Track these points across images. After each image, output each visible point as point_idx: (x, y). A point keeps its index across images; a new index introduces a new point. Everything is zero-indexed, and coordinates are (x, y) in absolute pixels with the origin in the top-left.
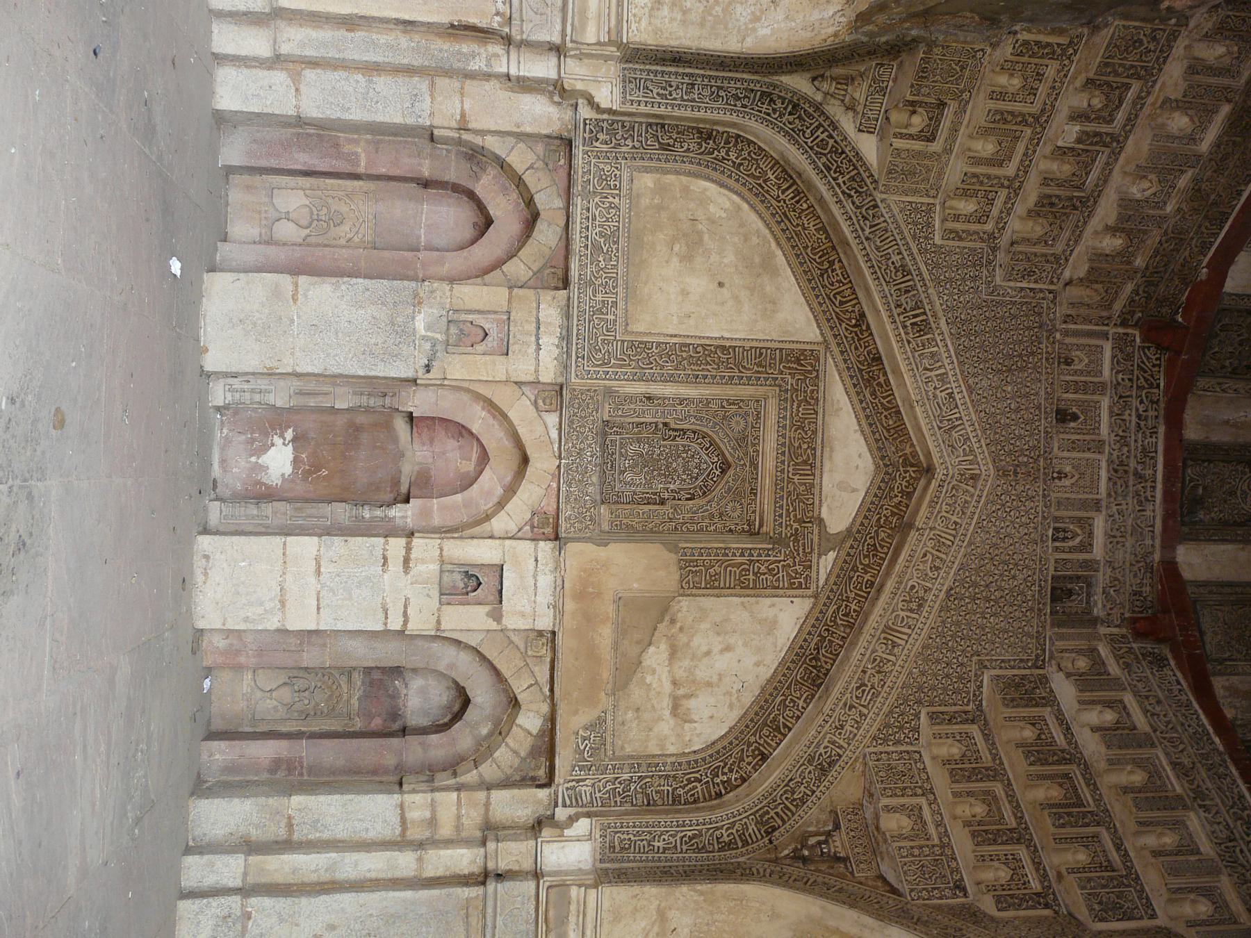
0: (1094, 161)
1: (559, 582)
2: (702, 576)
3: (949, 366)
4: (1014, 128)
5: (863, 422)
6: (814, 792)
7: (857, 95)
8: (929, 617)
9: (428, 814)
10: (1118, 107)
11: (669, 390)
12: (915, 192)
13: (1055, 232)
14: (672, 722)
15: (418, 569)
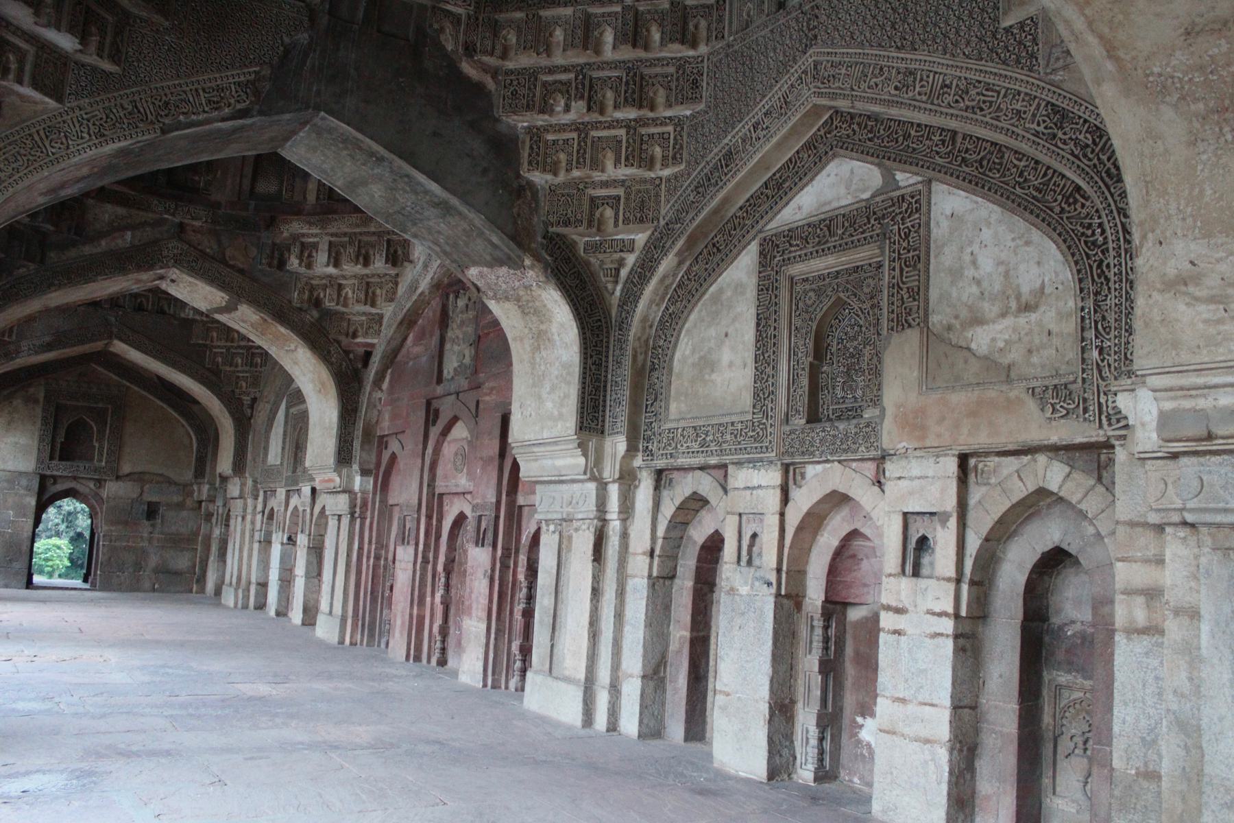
0: (599, 79)
1: (918, 453)
2: (910, 307)
3: (743, 128)
4: (589, 144)
5: (805, 180)
6: (1085, 121)
7: (608, 260)
8: (919, 59)
9: (1140, 600)
10: (560, 82)
11: (783, 366)
12: (657, 195)
13: (660, 79)
14: (1042, 309)
15: (905, 600)
